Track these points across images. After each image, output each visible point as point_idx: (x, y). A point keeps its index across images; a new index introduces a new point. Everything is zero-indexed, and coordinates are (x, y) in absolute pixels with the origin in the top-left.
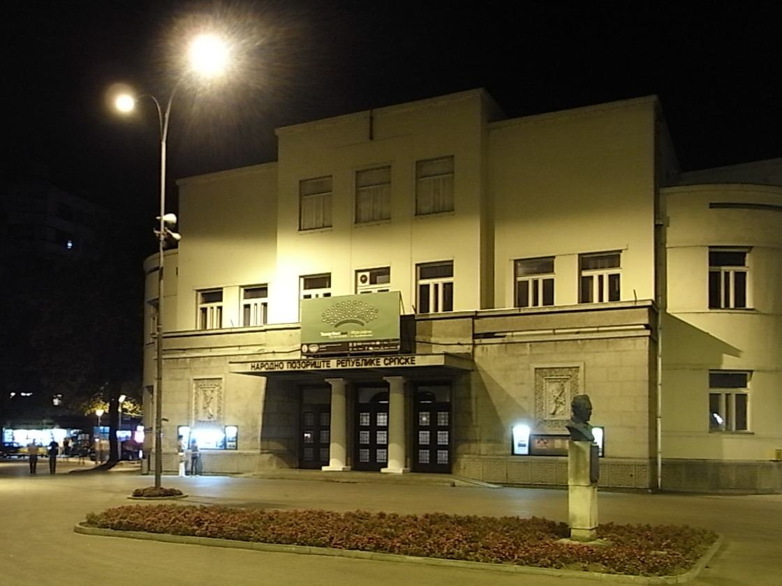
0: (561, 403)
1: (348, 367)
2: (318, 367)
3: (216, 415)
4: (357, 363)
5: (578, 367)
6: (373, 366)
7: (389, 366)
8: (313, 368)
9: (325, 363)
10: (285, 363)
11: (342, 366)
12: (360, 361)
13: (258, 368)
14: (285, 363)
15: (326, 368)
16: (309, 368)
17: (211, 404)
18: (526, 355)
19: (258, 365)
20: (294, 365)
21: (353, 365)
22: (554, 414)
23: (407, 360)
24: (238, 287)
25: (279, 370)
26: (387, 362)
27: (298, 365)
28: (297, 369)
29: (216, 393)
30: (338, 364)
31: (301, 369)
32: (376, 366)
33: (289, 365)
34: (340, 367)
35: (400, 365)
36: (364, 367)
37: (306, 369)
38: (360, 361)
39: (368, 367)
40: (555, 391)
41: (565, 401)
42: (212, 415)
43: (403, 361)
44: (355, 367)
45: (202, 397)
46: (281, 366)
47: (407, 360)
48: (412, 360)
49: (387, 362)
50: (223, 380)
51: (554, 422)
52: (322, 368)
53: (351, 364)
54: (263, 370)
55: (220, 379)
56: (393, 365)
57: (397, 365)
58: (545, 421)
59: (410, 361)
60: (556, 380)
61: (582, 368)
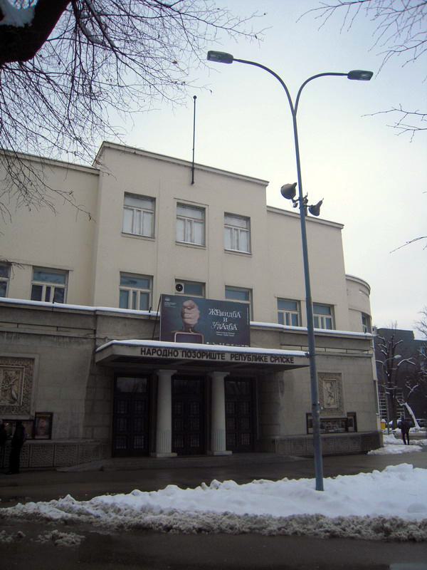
1: (241, 361)
2: (214, 358)
7: (274, 363)
8: (208, 359)
9: (220, 356)
10: (180, 354)
13: (149, 352)
14: (180, 354)
15: (220, 360)
17: (15, 388)
19: (149, 350)
20: (189, 354)
25: (173, 357)
26: (273, 359)
27: (193, 354)
28: (192, 358)
30: (231, 358)
31: (196, 358)
34: (233, 360)
36: (254, 362)
37: (201, 359)
39: (258, 362)
42: (14, 399)
44: (246, 361)
46: (176, 353)
49: (273, 359)
50: (37, 361)
52: (217, 360)
55: (33, 360)
56: (277, 363)
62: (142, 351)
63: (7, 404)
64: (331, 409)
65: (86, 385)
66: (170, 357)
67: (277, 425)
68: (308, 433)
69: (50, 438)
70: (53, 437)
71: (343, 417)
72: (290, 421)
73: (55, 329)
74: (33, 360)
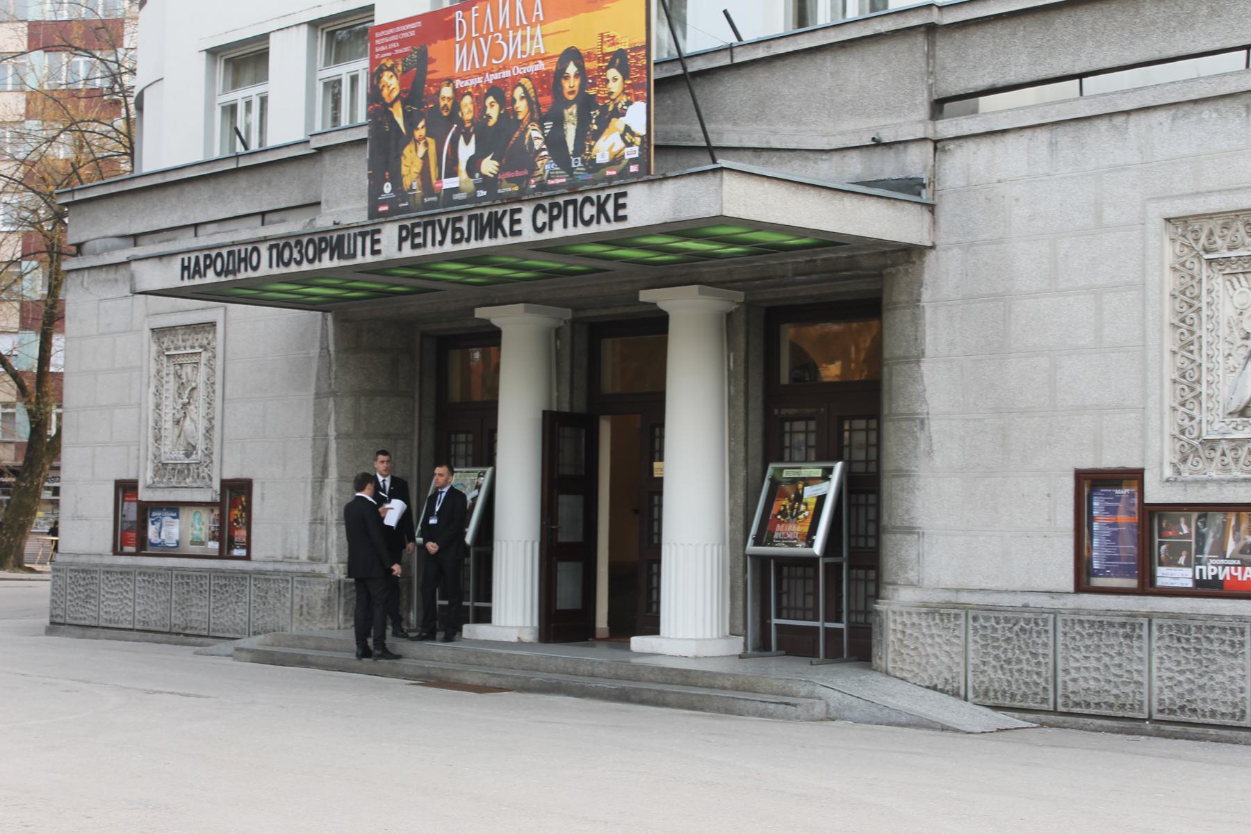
3: (201, 446)
4: (455, 230)
6: (500, 241)
7: (546, 235)
8: (336, 263)
9: (368, 240)
11: (414, 246)
12: (464, 225)
15: (369, 258)
16: (326, 262)
18: (1125, 167)
21: (441, 243)
23: (601, 209)
24: (305, 29)
27: (296, 255)
29: (203, 370)
30: (402, 240)
32: (511, 240)
33: (275, 252)
34: (407, 252)
35: (581, 230)
36: (474, 244)
37: (317, 265)
38: (464, 225)
39: (487, 242)
43: (589, 211)
45: (171, 385)
47: (601, 209)
48: (618, 207)
50: (220, 327)
52: (359, 260)
53: (438, 237)
54: (211, 277)
55: (213, 324)
56: (558, 231)
57: (572, 231)
58: (1212, 444)
59: (610, 208)
62: (184, 268)
63: (179, 456)
65: (312, 390)
66: (242, 275)
67: (910, 530)
68: (1082, 583)
69: (248, 558)
70: (254, 554)
72: (976, 522)
73: (258, 220)
74: (213, 324)
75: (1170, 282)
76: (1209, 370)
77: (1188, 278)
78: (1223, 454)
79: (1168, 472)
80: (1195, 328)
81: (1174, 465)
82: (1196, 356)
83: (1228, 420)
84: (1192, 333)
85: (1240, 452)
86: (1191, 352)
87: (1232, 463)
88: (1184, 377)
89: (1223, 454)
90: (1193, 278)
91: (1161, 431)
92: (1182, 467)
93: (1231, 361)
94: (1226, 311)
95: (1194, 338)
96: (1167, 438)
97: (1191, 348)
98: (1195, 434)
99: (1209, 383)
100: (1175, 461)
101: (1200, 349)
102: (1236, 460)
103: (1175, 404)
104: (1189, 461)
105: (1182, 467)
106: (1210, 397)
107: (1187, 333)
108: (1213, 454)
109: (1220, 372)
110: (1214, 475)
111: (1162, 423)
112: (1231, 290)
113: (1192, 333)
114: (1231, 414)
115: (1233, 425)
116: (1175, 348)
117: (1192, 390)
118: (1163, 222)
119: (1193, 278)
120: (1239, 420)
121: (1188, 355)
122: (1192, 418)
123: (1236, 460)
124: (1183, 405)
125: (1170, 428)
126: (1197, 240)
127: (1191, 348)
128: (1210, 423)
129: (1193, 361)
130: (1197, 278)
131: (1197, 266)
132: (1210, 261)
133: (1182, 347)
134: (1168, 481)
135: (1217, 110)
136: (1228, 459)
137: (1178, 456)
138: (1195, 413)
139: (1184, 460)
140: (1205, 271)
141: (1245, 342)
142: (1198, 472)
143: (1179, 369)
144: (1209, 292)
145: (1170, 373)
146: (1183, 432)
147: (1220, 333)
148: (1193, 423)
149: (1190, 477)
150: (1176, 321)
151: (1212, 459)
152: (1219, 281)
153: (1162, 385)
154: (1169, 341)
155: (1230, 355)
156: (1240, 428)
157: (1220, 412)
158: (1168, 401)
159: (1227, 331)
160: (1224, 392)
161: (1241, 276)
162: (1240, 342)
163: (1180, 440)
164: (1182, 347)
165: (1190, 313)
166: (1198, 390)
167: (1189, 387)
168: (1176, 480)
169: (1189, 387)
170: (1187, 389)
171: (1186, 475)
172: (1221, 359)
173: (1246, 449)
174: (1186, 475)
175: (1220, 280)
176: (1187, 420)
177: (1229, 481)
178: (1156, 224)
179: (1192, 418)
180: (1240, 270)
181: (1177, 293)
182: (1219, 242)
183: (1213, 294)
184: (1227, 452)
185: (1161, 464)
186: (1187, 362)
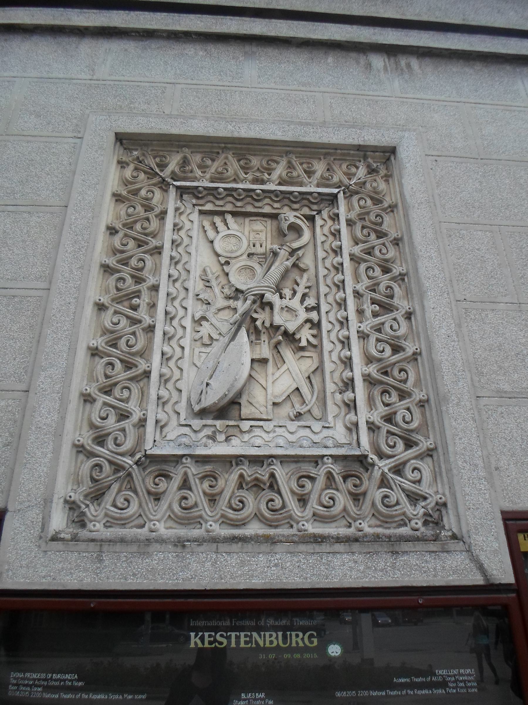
0: (290, 337)
5: (389, 153)
22: (227, 409)
40: (244, 261)
41: (317, 325)
51: (228, 481)
58: (161, 465)
60: (242, 206)
61: (409, 155)
64: (258, 473)
71: (449, 570)
75: (109, 213)
76: (167, 337)
77: (139, 208)
78: (185, 485)
79: (58, 521)
80: (145, 273)
81: (71, 506)
82: (143, 314)
83: (197, 423)
84: (138, 280)
85: (221, 483)
86: (135, 308)
87: (204, 502)
88: (114, 345)
89: (185, 485)
90: (148, 208)
91: (58, 435)
92: (91, 511)
93: (206, 329)
94: (201, 259)
95: (143, 287)
96: (66, 450)
97: (136, 301)
98: (128, 445)
99: (165, 358)
100: (76, 497)
101: (153, 306)
102: (213, 499)
103: (92, 390)
104: (109, 498)
105: (91, 511)
106: (164, 380)
107: (129, 280)
108: (163, 485)
109: (186, 342)
110: (163, 529)
111: (63, 418)
112: (211, 234)
113: (138, 280)
114: (203, 413)
115: (208, 431)
116: (105, 300)
117: (128, 366)
118: (112, 138)
119: (148, 208)
120: (219, 423)
121: (131, 313)
122: (123, 416)
123: (213, 499)
124: (107, 391)
125: (75, 431)
126: (162, 166)
127: (136, 301)
128: (161, 426)
129: (135, 322)
130: (157, 211)
131: (158, 194)
132: (182, 191)
133: (118, 300)
134: (55, 538)
135: (206, 50)
136: (197, 495)
137: (86, 486)
138: (132, 406)
139: (97, 496)
140: (172, 201)
141: (231, 302)
142: (123, 522)
143: (105, 331)
144: (177, 228)
145: (89, 336)
146: (100, 440)
147: (190, 285)
148: (125, 424)
149: (108, 533)
150: (112, 261)
151: (157, 497)
152: (192, 221)
153: (72, 350)
154: (96, 288)
155: (204, 318)
156: (221, 437)
157: (182, 407)
158: (79, 384)
159: (200, 285)
160: (189, 381)
161: (229, 217)
162: (221, 302)
163: (91, 455)
164: (118, 300)
165: (139, 253)
166: (143, 366)
167: (121, 362)
168: (75, 538)
169: (121, 362)
170: (118, 365)
171: (98, 528)
172: (188, 323)
173: (234, 477)
174: (98, 528)
175: (195, 216)
176: (112, 419)
177: (199, 541)
178: (100, 131)
179: (123, 416)
180: (229, 207)
181: (118, 225)
182: (198, 173)
183: (182, 233)
184: (194, 482)
185: (47, 502)
186: (124, 322)
